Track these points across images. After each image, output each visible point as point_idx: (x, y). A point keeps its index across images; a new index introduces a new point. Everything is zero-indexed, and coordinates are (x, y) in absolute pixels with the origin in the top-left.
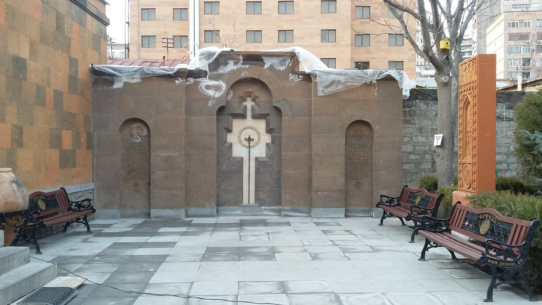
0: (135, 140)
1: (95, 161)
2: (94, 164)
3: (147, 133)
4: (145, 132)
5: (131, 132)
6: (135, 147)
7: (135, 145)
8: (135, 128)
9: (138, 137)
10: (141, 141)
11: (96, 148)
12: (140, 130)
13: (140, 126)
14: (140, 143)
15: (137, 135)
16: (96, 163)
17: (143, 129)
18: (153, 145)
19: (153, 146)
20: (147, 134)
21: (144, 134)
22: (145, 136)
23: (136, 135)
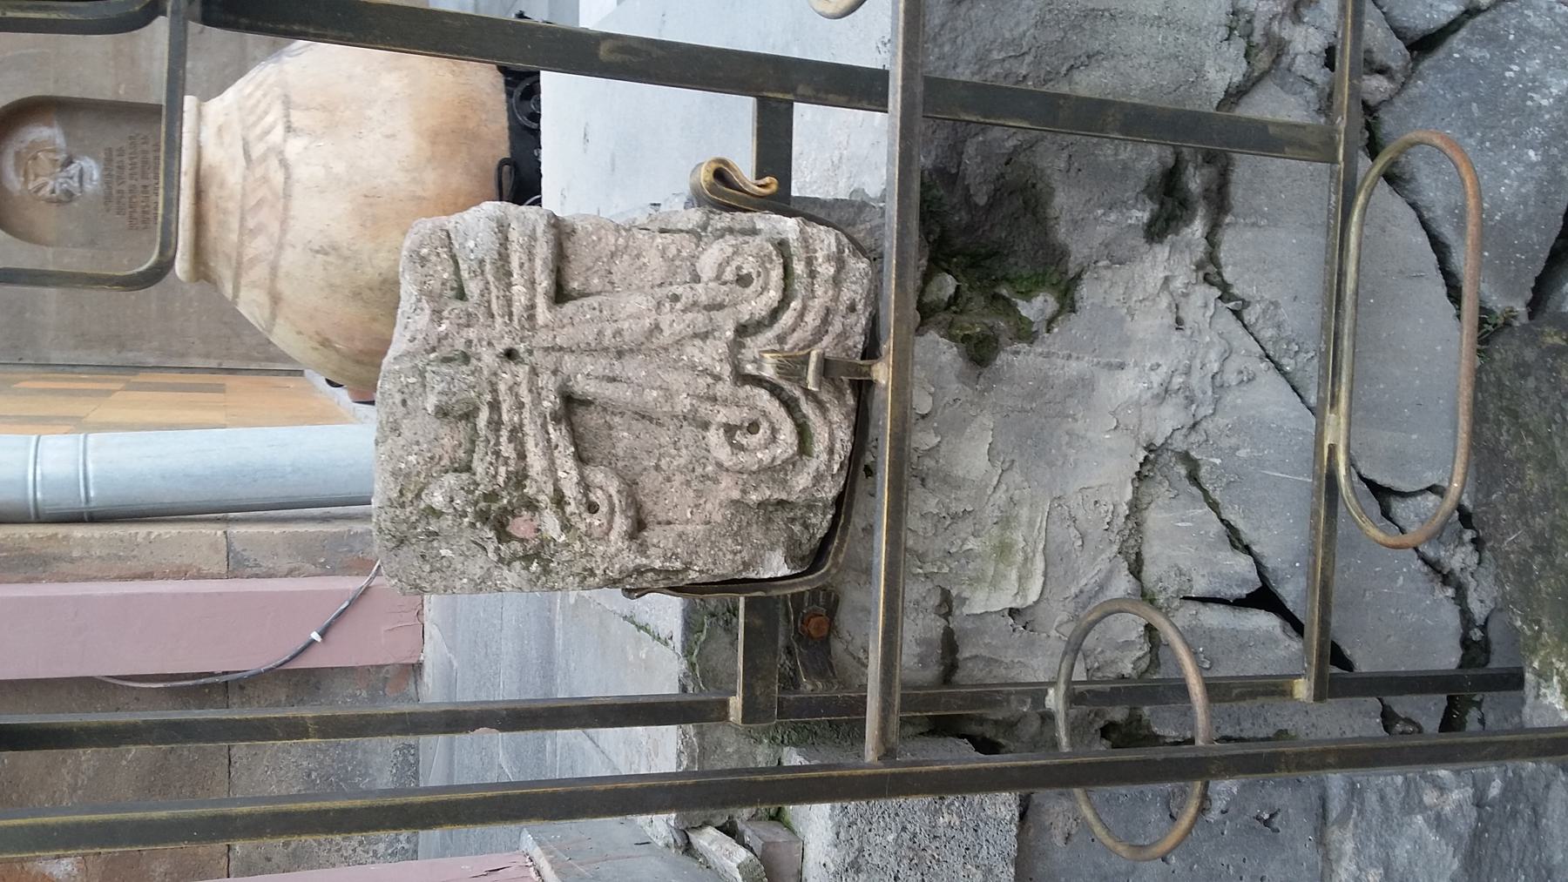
0: (88, 187)
1: (198, 363)
2: (213, 364)
3: (50, 125)
4: (45, 133)
5: (50, 201)
6: (125, 188)
7: (115, 187)
8: (26, 182)
9: (73, 169)
10: (96, 159)
11: (130, 355)
12: (35, 158)
13: (18, 154)
14: (109, 160)
15: (64, 174)
16: (207, 356)
17: (32, 142)
18: (117, 93)
19: (121, 92)
20: (56, 122)
21: (60, 141)
22: (67, 135)
23: (61, 180)
